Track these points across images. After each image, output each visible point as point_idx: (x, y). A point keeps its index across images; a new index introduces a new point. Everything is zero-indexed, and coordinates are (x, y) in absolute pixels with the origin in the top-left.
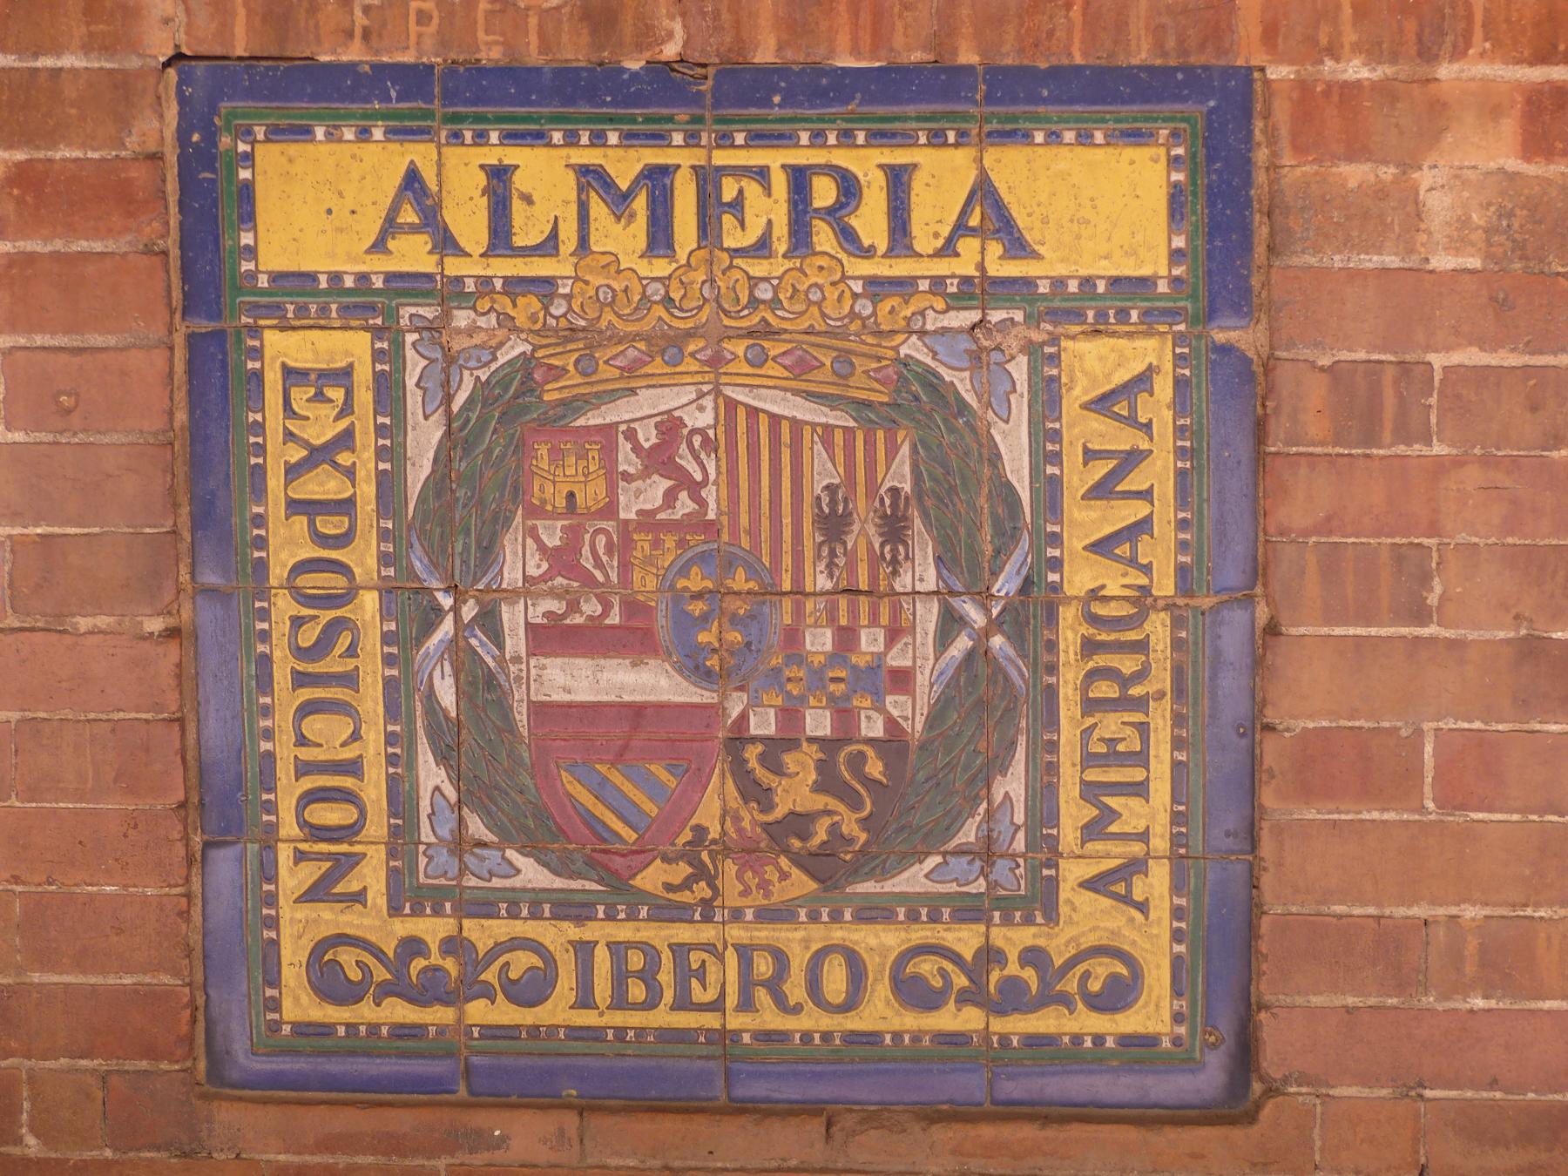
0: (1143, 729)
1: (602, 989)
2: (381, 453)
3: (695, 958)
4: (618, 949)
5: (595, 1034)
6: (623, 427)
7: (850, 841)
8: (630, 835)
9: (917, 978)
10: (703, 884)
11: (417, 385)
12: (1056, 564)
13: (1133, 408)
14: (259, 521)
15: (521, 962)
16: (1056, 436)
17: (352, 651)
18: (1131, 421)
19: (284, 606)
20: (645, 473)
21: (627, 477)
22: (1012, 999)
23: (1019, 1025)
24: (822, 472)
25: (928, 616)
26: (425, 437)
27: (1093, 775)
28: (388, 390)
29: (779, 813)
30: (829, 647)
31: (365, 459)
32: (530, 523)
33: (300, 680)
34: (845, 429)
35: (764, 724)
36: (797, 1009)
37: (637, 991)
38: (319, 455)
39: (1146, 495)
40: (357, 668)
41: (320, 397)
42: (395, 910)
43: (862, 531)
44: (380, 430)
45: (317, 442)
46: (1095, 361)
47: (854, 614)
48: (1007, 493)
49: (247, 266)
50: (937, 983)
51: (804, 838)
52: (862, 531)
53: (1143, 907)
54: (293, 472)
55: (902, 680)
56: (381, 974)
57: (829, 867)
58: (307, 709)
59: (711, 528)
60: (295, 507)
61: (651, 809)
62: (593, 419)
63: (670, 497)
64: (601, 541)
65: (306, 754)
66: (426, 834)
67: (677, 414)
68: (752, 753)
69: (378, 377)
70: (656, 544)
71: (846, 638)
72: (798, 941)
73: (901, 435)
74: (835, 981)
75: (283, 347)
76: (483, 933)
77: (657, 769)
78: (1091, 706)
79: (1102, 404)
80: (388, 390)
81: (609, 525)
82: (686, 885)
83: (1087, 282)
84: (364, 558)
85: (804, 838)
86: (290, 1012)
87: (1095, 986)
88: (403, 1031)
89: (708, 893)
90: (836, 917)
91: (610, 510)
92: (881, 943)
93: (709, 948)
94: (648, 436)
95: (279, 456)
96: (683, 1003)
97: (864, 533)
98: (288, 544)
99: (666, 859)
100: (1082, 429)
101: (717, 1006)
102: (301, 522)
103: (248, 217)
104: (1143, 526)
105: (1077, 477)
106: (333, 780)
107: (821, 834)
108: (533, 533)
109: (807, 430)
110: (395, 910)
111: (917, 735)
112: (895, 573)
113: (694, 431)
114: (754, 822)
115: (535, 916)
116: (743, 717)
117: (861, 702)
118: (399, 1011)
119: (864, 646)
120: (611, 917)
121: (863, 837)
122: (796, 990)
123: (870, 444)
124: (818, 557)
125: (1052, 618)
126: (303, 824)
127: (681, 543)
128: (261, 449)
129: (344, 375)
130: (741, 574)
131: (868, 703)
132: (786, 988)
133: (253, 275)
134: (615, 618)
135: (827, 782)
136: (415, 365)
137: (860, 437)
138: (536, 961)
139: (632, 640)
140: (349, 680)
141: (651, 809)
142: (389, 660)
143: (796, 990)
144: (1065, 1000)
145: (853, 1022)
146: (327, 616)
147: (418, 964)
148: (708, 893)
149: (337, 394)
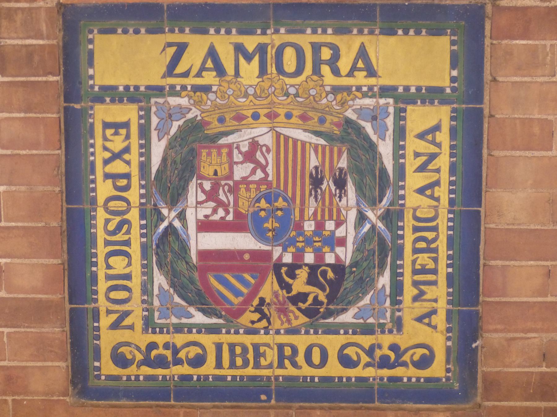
0: (435, 260)
1: (226, 361)
2: (141, 155)
3: (262, 349)
4: (232, 347)
5: (223, 378)
6: (235, 145)
7: (321, 303)
8: (236, 301)
9: (348, 356)
10: (265, 320)
11: (155, 130)
12: (403, 197)
13: (434, 138)
14: (94, 181)
15: (194, 351)
16: (403, 148)
17: (128, 232)
18: (433, 142)
19: (101, 215)
20: (242, 163)
21: (237, 163)
22: (385, 363)
23: (386, 373)
24: (313, 161)
25: (352, 216)
26: (158, 149)
27: (417, 278)
28: (144, 132)
29: (294, 292)
30: (313, 228)
31: (134, 157)
32: (199, 181)
33: (107, 243)
34: (322, 145)
35: (288, 259)
36: (300, 368)
37: (239, 361)
38: (116, 156)
39: (438, 171)
40: (130, 238)
41: (116, 133)
42: (145, 330)
43: (328, 184)
44: (141, 146)
45: (117, 150)
46: (419, 117)
47: (323, 216)
48: (383, 170)
49: (91, 82)
50: (355, 358)
51: (304, 302)
52: (328, 184)
53: (435, 327)
54: (106, 162)
55: (342, 242)
56: (139, 357)
57: (309, 313)
58: (110, 254)
59: (269, 185)
60: (107, 176)
61: (245, 291)
62: (223, 141)
63: (253, 172)
64: (226, 188)
65: (111, 272)
66: (156, 303)
67: (256, 139)
68: (284, 270)
69: (140, 126)
70: (248, 190)
71: (320, 226)
72: (301, 342)
73: (344, 148)
74: (316, 358)
75: (103, 113)
76: (180, 339)
77: (247, 276)
78: (416, 251)
79: (421, 136)
80: (144, 132)
81: (231, 183)
82: (260, 320)
83: (419, 89)
84: (134, 195)
85: (304, 302)
86: (104, 371)
87: (416, 358)
88: (148, 378)
89: (267, 325)
90: (316, 333)
91: (230, 176)
92: (333, 343)
93: (268, 345)
94: (245, 148)
95: (100, 156)
96: (257, 365)
97: (328, 185)
98: (104, 190)
99: (250, 311)
100: (412, 145)
101: (270, 366)
102: (110, 182)
103: (91, 64)
104: (437, 183)
105: (411, 164)
106: (120, 282)
107: (310, 299)
108: (201, 185)
109: (308, 145)
110: (145, 330)
111: (348, 263)
112: (340, 201)
113: (262, 146)
114: (283, 296)
115: (199, 332)
116: (280, 258)
117: (326, 249)
118: (146, 370)
119: (327, 228)
120: (228, 332)
121: (325, 301)
122: (300, 359)
123: (331, 152)
124: (311, 194)
125: (400, 215)
126: (108, 299)
127: (258, 189)
128: (93, 154)
129: (126, 125)
130: (281, 199)
131: (328, 250)
132: (297, 359)
133: (92, 87)
134: (230, 217)
135: (312, 280)
136: (155, 120)
137: (327, 148)
138: (200, 351)
139: (237, 226)
140: (127, 243)
141: (245, 291)
142: (142, 235)
143: (300, 359)
144: (404, 364)
145: (322, 372)
146: (118, 219)
147: (154, 353)
148: (267, 325)
149: (123, 131)
